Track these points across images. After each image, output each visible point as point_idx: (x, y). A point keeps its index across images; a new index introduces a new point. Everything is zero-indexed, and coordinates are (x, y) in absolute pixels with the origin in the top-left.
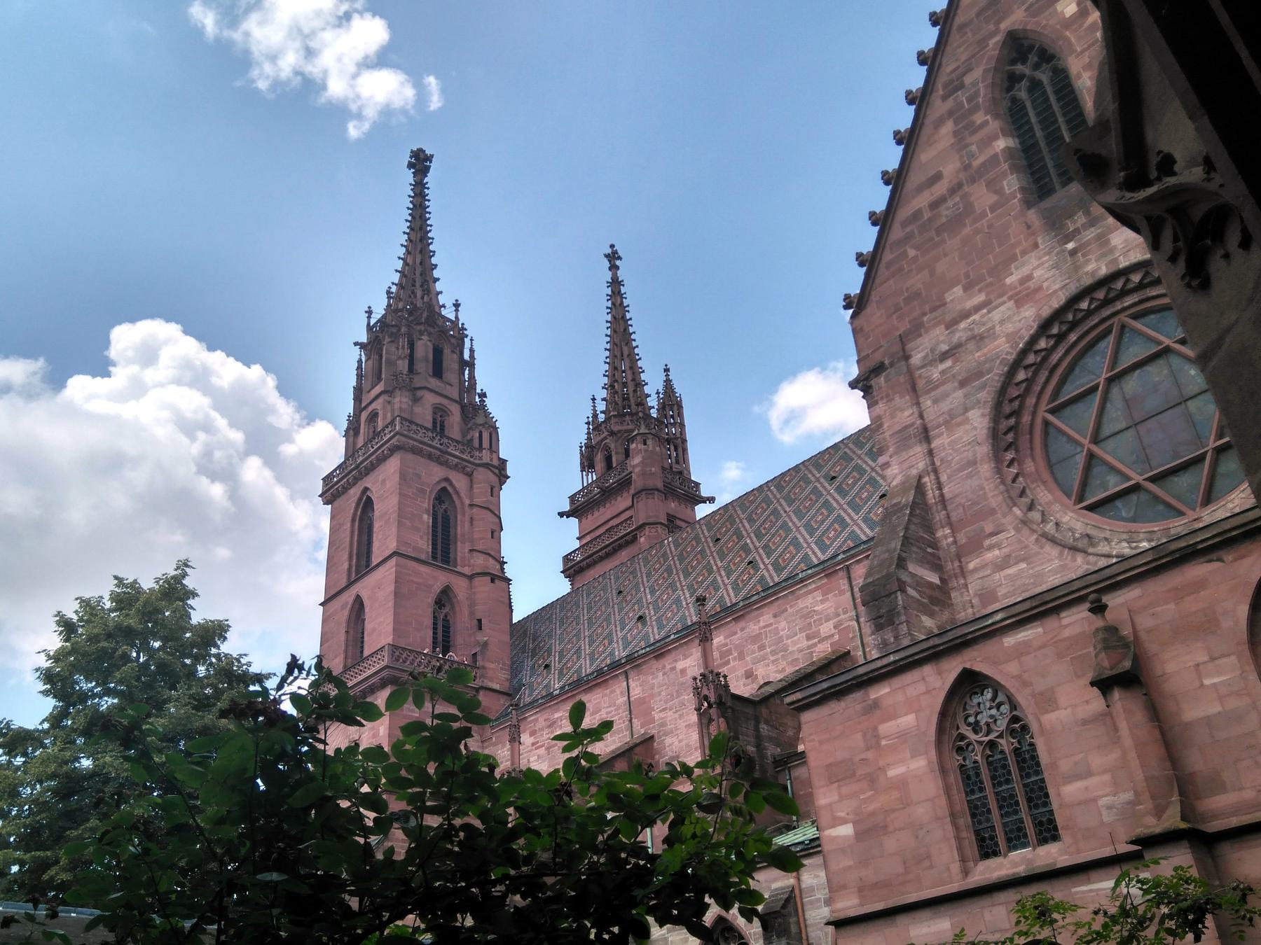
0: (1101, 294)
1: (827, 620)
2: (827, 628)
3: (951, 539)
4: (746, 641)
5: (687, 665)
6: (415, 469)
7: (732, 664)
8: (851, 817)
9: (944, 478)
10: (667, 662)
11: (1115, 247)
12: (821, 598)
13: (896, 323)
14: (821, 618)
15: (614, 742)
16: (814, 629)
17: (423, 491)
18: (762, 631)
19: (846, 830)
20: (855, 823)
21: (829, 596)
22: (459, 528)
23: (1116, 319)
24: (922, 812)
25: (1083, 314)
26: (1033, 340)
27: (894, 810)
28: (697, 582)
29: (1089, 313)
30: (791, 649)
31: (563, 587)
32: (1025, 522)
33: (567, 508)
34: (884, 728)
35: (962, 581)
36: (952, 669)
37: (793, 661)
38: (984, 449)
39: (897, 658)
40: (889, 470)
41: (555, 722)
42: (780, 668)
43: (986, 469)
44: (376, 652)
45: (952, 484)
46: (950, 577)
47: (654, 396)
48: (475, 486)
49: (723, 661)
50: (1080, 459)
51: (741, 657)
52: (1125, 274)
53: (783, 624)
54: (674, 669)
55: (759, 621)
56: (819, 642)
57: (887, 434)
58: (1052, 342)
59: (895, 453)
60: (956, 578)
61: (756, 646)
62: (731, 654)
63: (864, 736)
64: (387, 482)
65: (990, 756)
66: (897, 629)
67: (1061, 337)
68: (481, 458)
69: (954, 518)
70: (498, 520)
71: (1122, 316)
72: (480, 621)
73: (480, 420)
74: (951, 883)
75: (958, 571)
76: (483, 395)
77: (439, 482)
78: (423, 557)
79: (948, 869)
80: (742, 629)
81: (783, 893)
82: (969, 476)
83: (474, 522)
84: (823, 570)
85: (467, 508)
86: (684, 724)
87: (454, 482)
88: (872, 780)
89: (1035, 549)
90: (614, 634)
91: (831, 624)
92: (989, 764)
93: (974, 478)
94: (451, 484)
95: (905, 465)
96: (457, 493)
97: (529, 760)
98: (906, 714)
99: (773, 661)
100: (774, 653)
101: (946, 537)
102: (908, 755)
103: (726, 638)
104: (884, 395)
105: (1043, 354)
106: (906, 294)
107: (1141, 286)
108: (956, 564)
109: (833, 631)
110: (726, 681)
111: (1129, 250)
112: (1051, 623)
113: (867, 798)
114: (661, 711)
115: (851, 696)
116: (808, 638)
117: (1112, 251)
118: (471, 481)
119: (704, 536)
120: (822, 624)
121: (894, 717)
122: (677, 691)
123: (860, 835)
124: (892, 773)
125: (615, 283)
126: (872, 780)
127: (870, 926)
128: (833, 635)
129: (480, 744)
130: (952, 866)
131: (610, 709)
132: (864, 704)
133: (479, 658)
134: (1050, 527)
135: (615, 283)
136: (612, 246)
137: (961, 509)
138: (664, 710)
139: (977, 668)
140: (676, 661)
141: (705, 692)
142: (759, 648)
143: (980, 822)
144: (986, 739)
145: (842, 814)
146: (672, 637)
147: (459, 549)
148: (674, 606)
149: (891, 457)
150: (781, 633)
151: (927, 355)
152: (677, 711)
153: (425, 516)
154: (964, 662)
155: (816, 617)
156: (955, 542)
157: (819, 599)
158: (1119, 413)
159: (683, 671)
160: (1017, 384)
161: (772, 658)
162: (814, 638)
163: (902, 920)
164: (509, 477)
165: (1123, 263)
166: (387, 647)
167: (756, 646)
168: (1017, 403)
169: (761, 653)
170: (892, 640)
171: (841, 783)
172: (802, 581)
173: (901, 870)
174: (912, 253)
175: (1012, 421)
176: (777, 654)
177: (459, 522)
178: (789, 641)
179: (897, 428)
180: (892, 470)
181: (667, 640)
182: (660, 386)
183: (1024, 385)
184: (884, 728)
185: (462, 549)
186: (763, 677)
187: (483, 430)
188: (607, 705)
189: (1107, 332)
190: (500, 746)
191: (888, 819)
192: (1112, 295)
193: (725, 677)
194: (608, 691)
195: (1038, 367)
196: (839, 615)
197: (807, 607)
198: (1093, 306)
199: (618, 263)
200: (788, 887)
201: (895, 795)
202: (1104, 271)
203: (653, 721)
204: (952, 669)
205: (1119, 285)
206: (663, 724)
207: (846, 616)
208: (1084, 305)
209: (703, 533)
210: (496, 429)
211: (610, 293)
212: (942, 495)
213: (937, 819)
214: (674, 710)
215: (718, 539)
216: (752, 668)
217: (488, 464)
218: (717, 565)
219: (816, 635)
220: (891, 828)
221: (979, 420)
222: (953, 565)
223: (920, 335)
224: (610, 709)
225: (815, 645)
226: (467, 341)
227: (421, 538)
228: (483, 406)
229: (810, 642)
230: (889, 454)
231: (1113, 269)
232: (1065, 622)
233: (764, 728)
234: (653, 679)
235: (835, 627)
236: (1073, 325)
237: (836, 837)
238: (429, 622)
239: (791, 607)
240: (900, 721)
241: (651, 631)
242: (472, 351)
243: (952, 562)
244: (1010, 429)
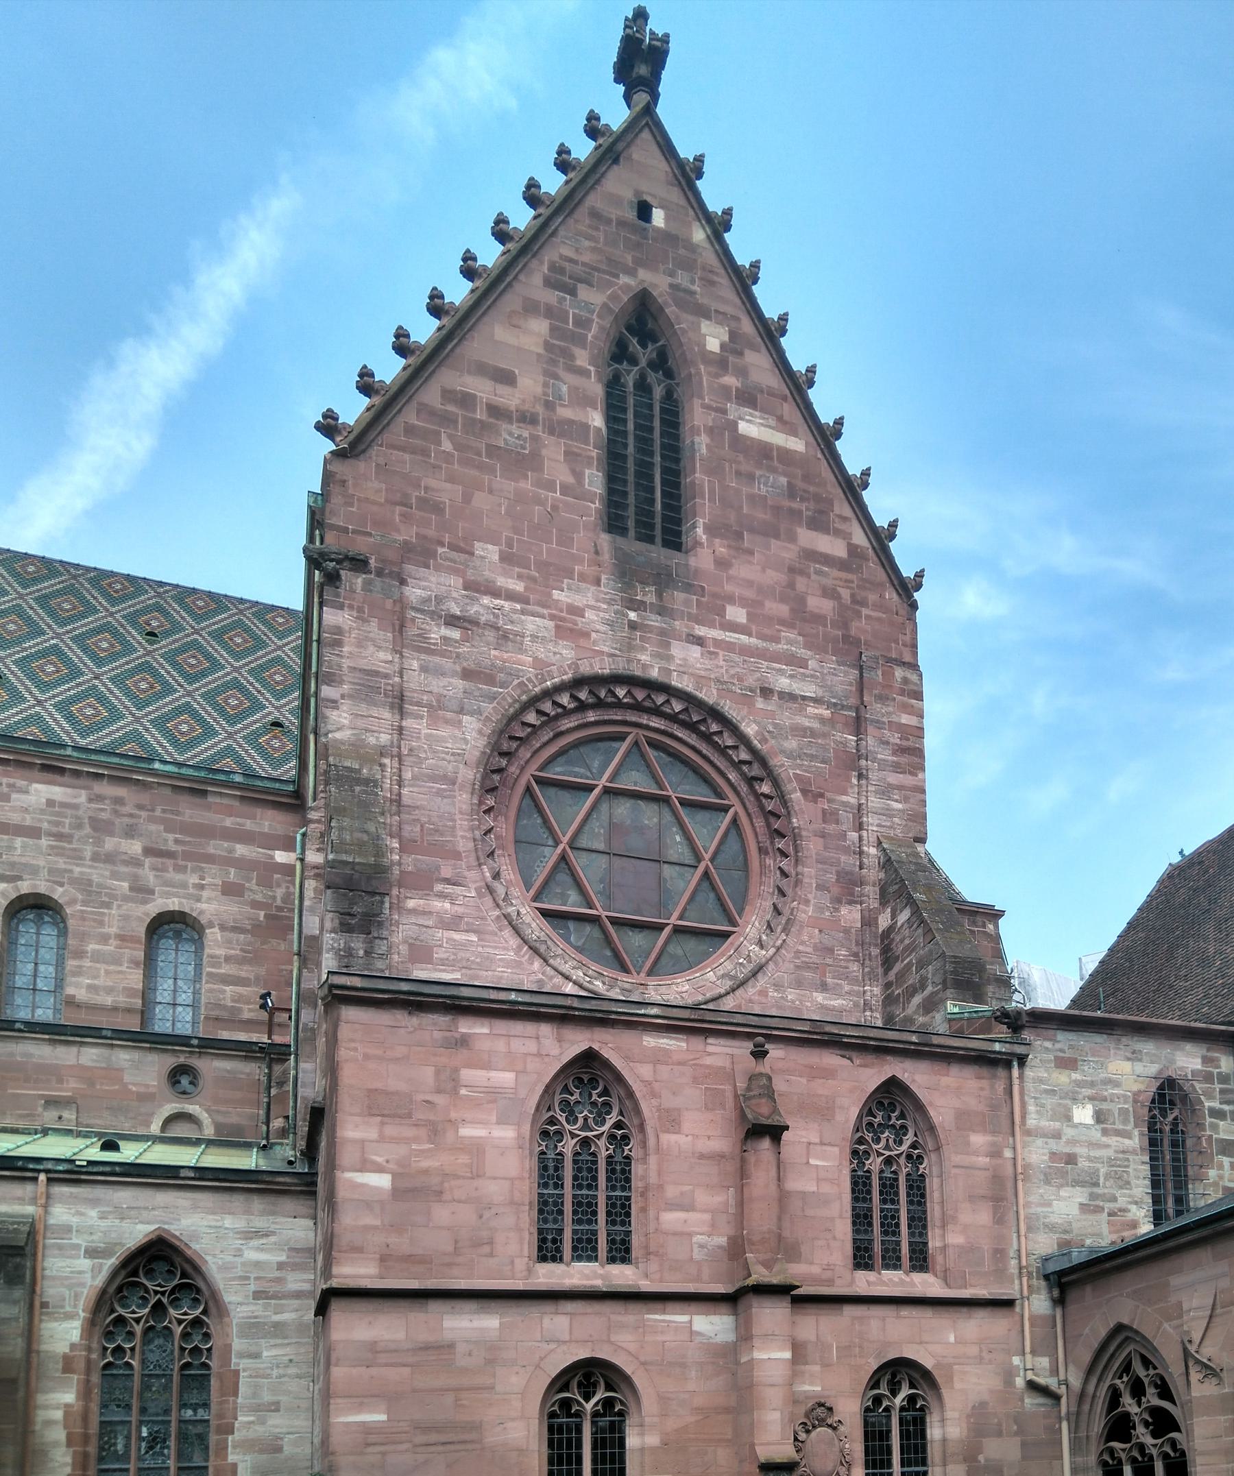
0: (640, 695)
9: (407, 775)
11: (673, 657)
23: (635, 731)
24: (494, 1190)
25: (613, 700)
26: (559, 689)
27: (457, 1177)
29: (619, 705)
32: (491, 890)
34: (467, 1075)
36: (577, 1041)
38: (468, 774)
43: (464, 800)
45: (415, 789)
50: (552, 855)
52: (669, 694)
58: (572, 706)
65: (579, 1154)
66: (371, 942)
67: (582, 707)
69: (405, 834)
71: (641, 732)
79: (512, 1262)
82: (439, 793)
88: (435, 1131)
89: (493, 927)
92: (575, 1162)
93: (445, 800)
102: (494, 1119)
105: (560, 710)
107: (673, 718)
111: (684, 673)
112: (697, 1043)
115: (435, 1016)
117: (669, 658)
124: (465, 1131)
126: (435, 1131)
127: (387, 1304)
130: (517, 1261)
134: (510, 910)
137: (418, 829)
139: (607, 1053)
143: (545, 1221)
154: (593, 1041)
156: (400, 863)
158: (602, 831)
160: (524, 724)
163: (435, 1306)
165: (675, 683)
168: (514, 745)
170: (361, 953)
173: (450, 1249)
175: (504, 762)
183: (529, 730)
184: (467, 1075)
189: (621, 738)
191: (446, 1185)
192: (647, 704)
195: (550, 720)
198: (625, 700)
201: (464, 1159)
202: (654, 673)
204: (577, 1041)
205: (660, 699)
208: (621, 692)
212: (399, 794)
213: (512, 1203)
220: (447, 1196)
221: (474, 734)
231: (663, 679)
232: (710, 1049)
236: (600, 704)
240: (493, 1074)
244: (500, 771)
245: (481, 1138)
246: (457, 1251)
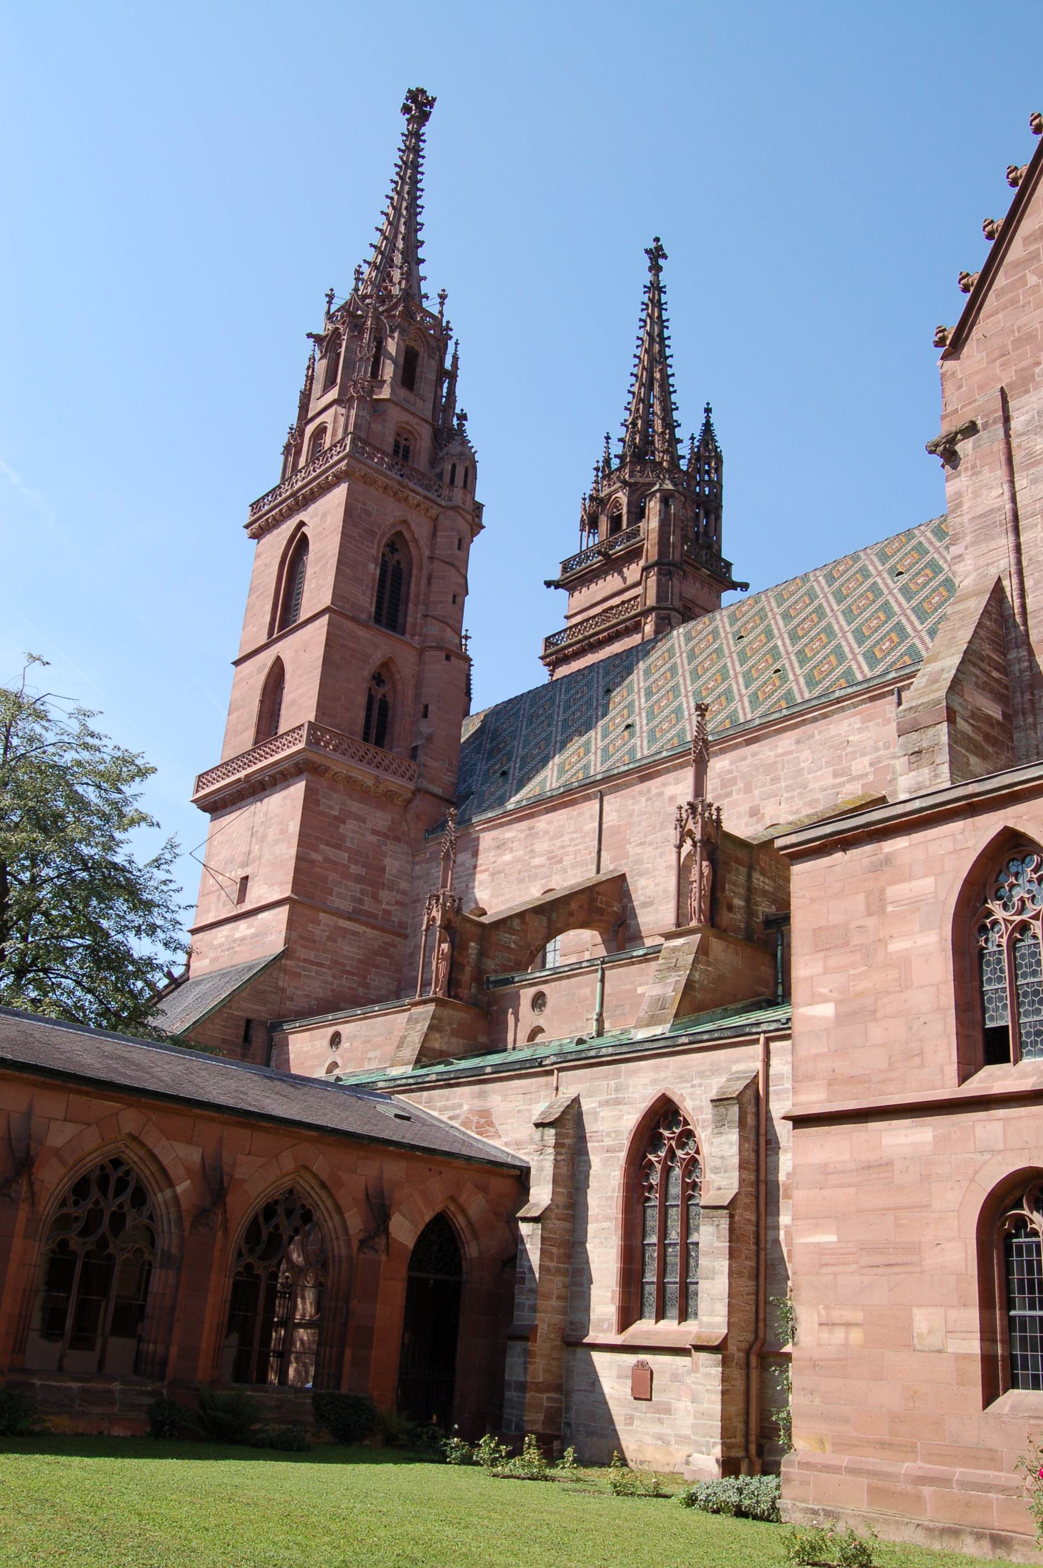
1: (863, 755)
2: (861, 765)
3: (1026, 664)
4: (757, 769)
5: (678, 792)
6: (365, 505)
7: (735, 796)
8: (835, 994)
10: (653, 784)
12: (859, 725)
13: (998, 371)
14: (855, 752)
15: (575, 876)
16: (844, 764)
17: (373, 534)
18: (779, 759)
19: (826, 1010)
20: (838, 1003)
21: (870, 724)
22: (413, 586)
27: (888, 993)
28: (707, 689)
30: (811, 786)
31: (539, 676)
33: (556, 575)
34: (893, 891)
35: (1031, 720)
37: (811, 801)
39: (924, 805)
40: (962, 564)
41: (504, 844)
42: (794, 809)
44: (293, 731)
46: (1016, 712)
47: (687, 443)
48: (439, 534)
49: (724, 791)
51: (748, 789)
53: (807, 753)
54: (661, 794)
55: (777, 746)
56: (848, 781)
57: (966, 519)
59: (973, 544)
60: (1024, 714)
61: (768, 778)
62: (736, 784)
63: (867, 897)
64: (329, 517)
68: (450, 499)
70: (463, 581)
72: (426, 707)
73: (454, 448)
74: (943, 1087)
75: (1027, 706)
76: (463, 417)
77: (394, 525)
78: (363, 616)
80: (754, 755)
81: (747, 1078)
83: (433, 580)
84: (867, 691)
85: (425, 561)
86: (665, 865)
87: (413, 526)
90: (593, 743)
91: (866, 760)
94: (409, 528)
95: (982, 562)
96: (416, 541)
97: (467, 885)
98: (924, 876)
99: (787, 799)
100: (789, 788)
101: (1019, 661)
103: (732, 763)
104: (969, 465)
106: (1017, 335)
108: (1028, 696)
109: (868, 769)
110: (718, 815)
113: (859, 974)
114: (638, 845)
116: (836, 775)
118: (435, 528)
119: (725, 630)
120: (856, 759)
121: (910, 879)
122: (662, 823)
123: (840, 1019)
124: (894, 947)
125: (656, 288)
128: (867, 774)
129: (411, 858)
131: (575, 835)
132: (874, 858)
133: (420, 752)
135: (656, 288)
136: (657, 240)
138: (642, 844)
139: (1021, 828)
140: (665, 785)
141: (690, 825)
142: (772, 780)
144: (1018, 918)
145: (824, 991)
146: (664, 754)
147: (410, 612)
148: (673, 716)
149: (966, 548)
150: (803, 765)
151: (1033, 417)
152: (657, 848)
153: (372, 566)
154: (1007, 819)
155: (849, 749)
157: (856, 726)
159: (672, 799)
161: (786, 795)
162: (842, 775)
164: (484, 527)
166: (306, 725)
167: (768, 778)
169: (773, 787)
171: (828, 953)
172: (838, 701)
174: (1032, 280)
176: (793, 790)
177: (413, 578)
178: (811, 776)
179: (980, 510)
180: (966, 565)
181: (657, 757)
182: (697, 431)
184: (893, 891)
185: (413, 614)
186: (771, 818)
187: (457, 462)
188: (572, 829)
190: (434, 863)
191: (879, 1003)
193: (718, 809)
194: (575, 813)
196: (878, 750)
197: (840, 734)
199: (661, 262)
200: (752, 1072)
203: (626, 856)
206: (638, 862)
207: (887, 752)
209: (724, 627)
210: (474, 463)
211: (646, 301)
213: (938, 1009)
214: (655, 846)
215: (741, 637)
216: (759, 805)
217: (458, 507)
218: (735, 670)
219: (846, 772)
220: (879, 1015)
222: (1022, 697)
223: (1027, 392)
224: (575, 835)
225: (842, 784)
226: (451, 344)
227: (364, 594)
228: (461, 430)
229: (838, 780)
230: (964, 544)
233: (758, 879)
234: (633, 804)
235: (871, 765)
237: (813, 1017)
238: (362, 700)
239: (820, 732)
241: (639, 744)
242: (455, 358)
243: (1022, 694)
245: (906, 950)
246: (891, 1067)
